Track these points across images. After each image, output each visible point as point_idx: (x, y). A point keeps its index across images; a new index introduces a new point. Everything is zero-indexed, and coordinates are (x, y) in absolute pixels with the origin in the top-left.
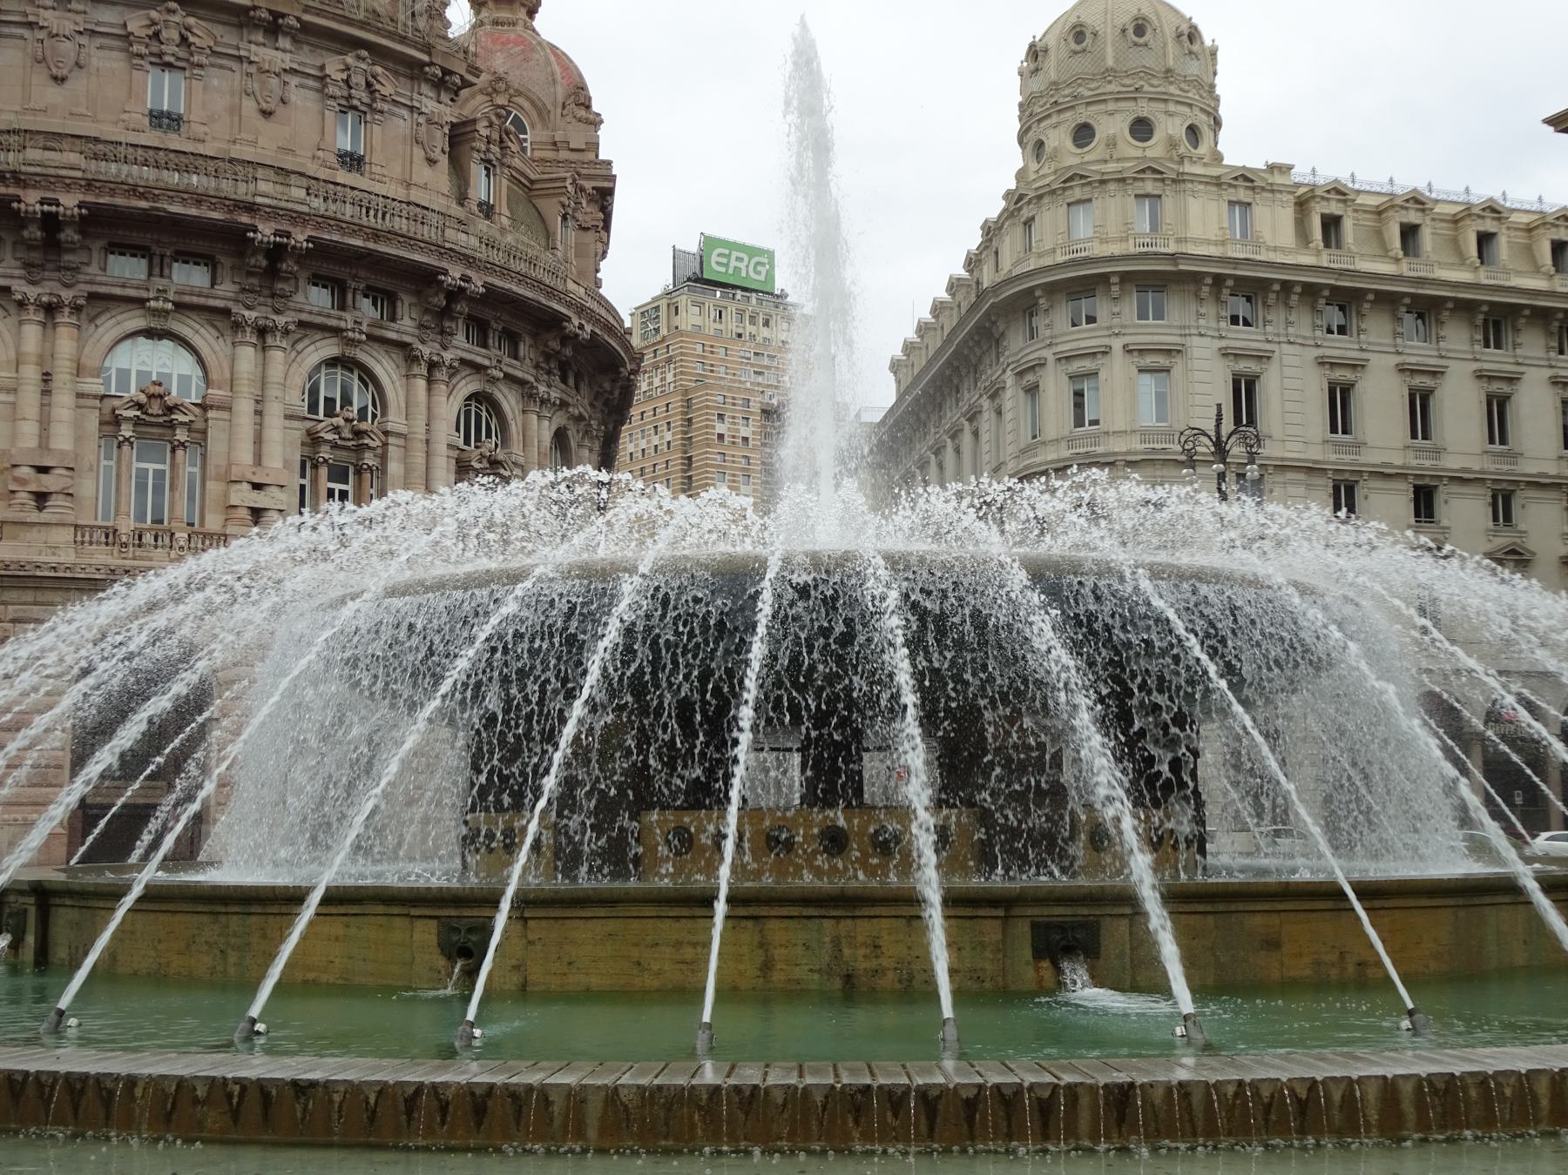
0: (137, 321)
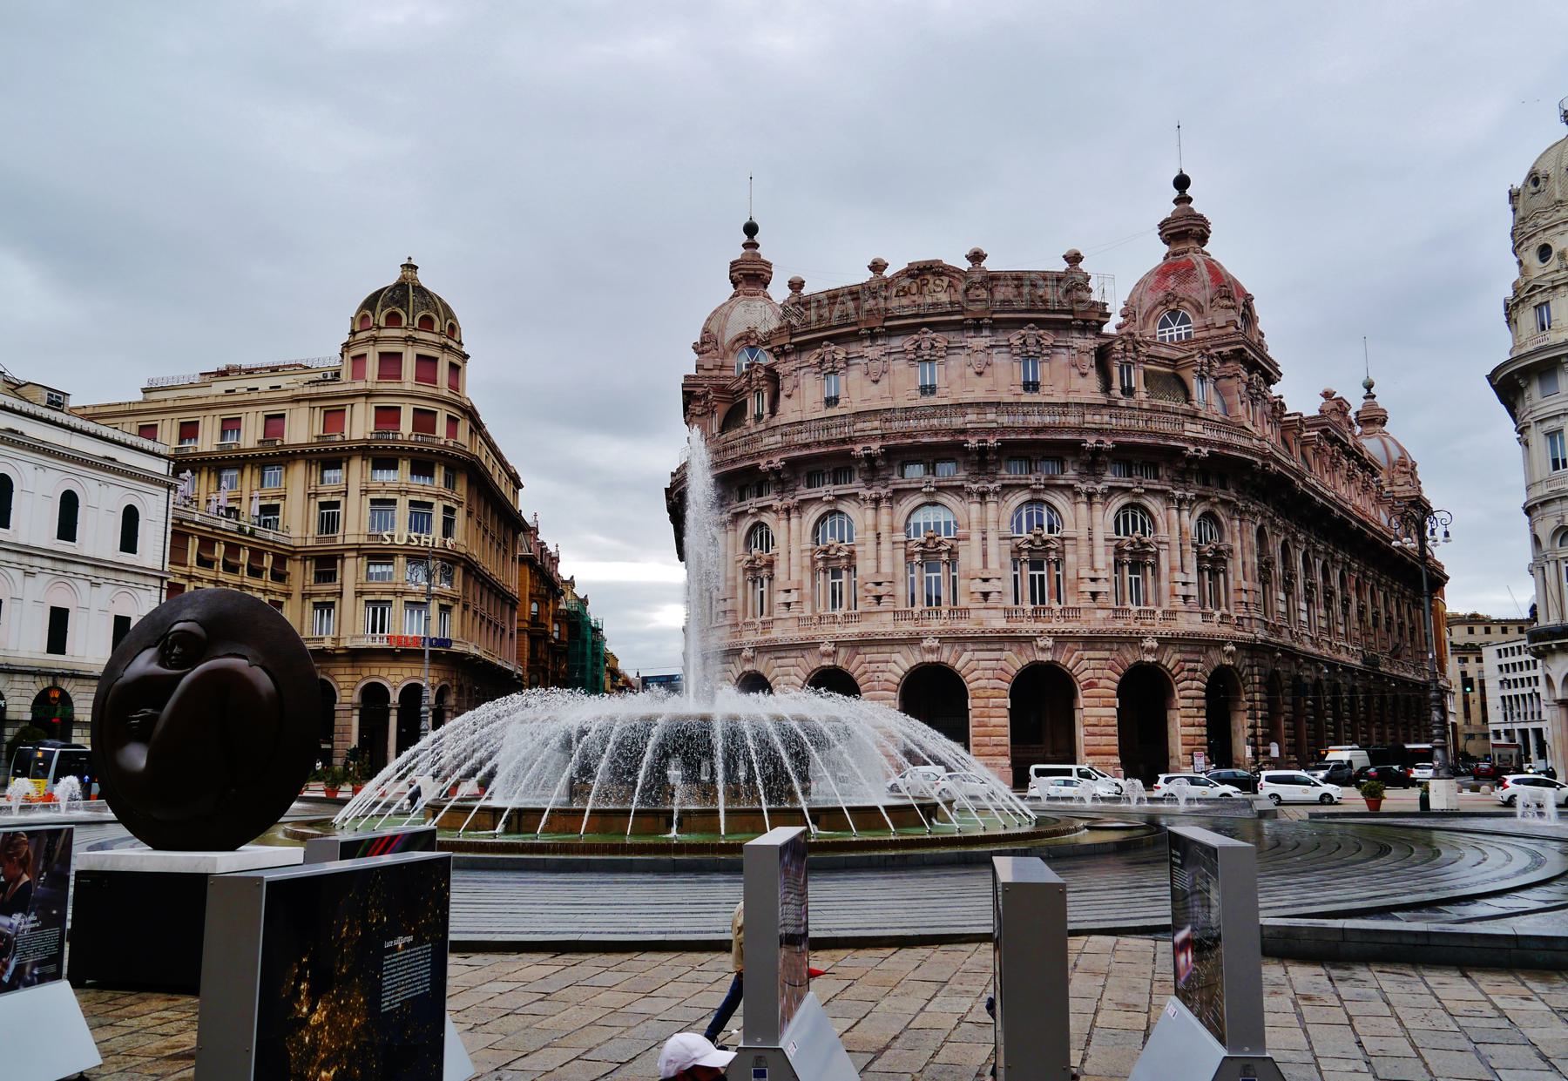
0: (918, 499)
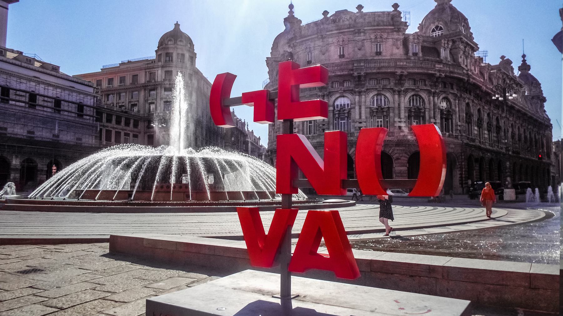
0: (338, 95)
